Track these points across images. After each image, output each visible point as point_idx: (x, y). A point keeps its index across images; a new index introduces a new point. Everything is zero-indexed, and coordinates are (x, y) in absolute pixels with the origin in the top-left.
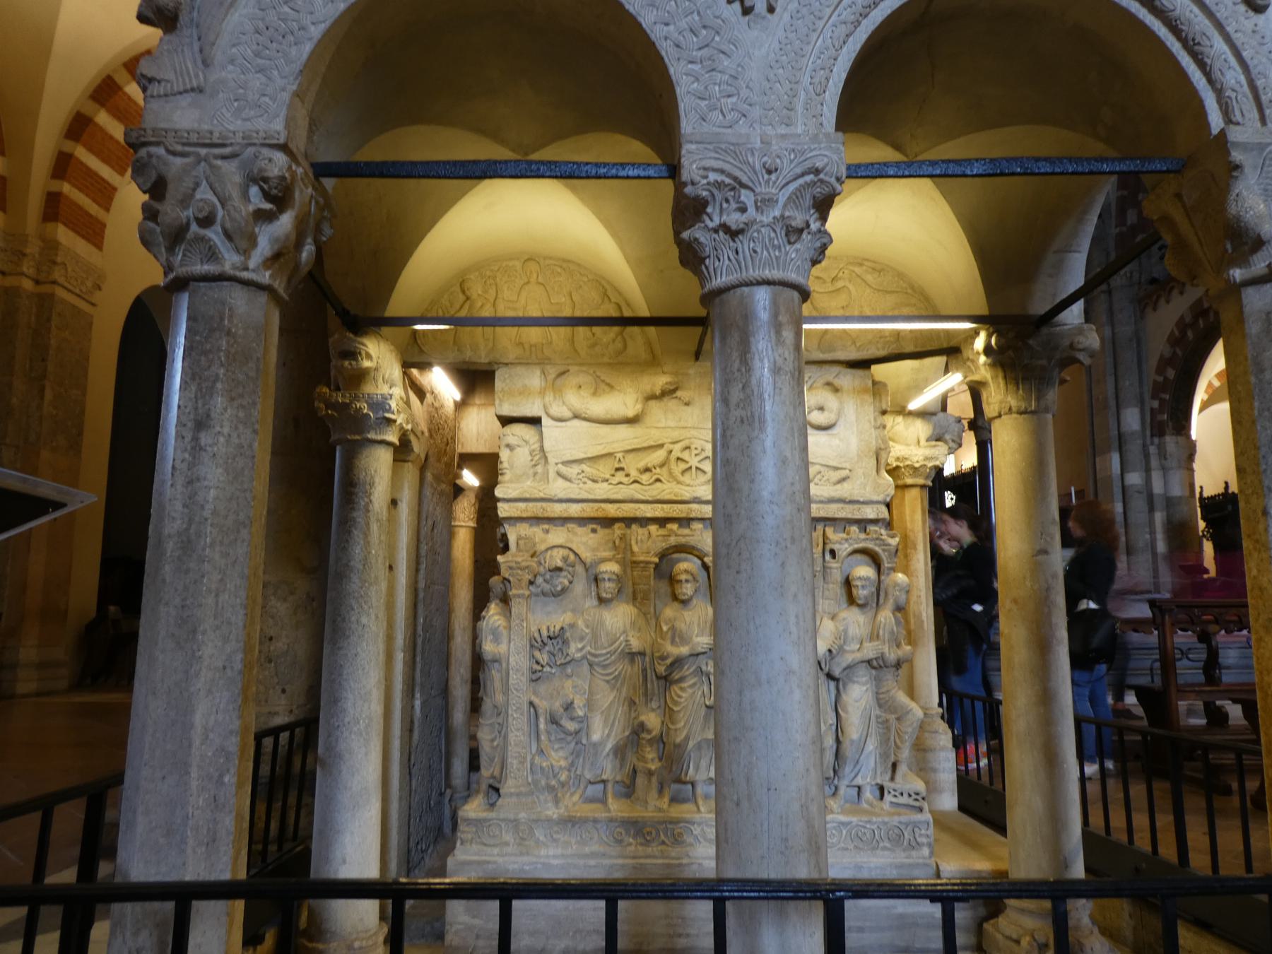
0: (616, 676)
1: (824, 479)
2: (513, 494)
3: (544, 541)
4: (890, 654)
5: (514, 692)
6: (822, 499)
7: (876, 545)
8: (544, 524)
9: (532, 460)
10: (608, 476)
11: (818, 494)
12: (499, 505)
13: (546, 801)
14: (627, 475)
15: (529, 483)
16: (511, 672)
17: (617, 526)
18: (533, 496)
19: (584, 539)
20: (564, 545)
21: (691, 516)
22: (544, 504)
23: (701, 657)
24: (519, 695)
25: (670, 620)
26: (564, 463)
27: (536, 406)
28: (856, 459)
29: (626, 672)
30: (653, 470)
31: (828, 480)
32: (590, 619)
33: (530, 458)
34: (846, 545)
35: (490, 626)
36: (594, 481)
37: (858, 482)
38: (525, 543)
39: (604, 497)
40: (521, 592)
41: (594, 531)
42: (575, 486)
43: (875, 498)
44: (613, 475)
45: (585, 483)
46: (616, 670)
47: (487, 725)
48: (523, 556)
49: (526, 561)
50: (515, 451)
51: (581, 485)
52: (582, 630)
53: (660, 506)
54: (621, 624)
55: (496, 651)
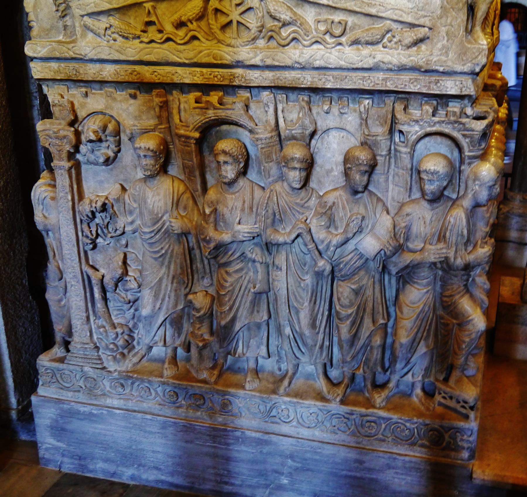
0: (163, 255)
1: (395, 40)
2: (43, 52)
3: (83, 105)
4: (455, 258)
6: (390, 66)
7: (454, 128)
9: (57, 10)
10: (138, 33)
11: (385, 60)
12: (32, 65)
14: (160, 31)
17: (155, 92)
21: (235, 84)
23: (245, 243)
25: (212, 202)
28: (439, 12)
29: (172, 251)
30: (189, 24)
31: (400, 41)
32: (136, 194)
34: (417, 128)
37: (439, 46)
38: (60, 110)
41: (134, 97)
43: (459, 68)
44: (144, 31)
46: (162, 248)
48: (60, 124)
53: (198, 69)
54: (161, 204)
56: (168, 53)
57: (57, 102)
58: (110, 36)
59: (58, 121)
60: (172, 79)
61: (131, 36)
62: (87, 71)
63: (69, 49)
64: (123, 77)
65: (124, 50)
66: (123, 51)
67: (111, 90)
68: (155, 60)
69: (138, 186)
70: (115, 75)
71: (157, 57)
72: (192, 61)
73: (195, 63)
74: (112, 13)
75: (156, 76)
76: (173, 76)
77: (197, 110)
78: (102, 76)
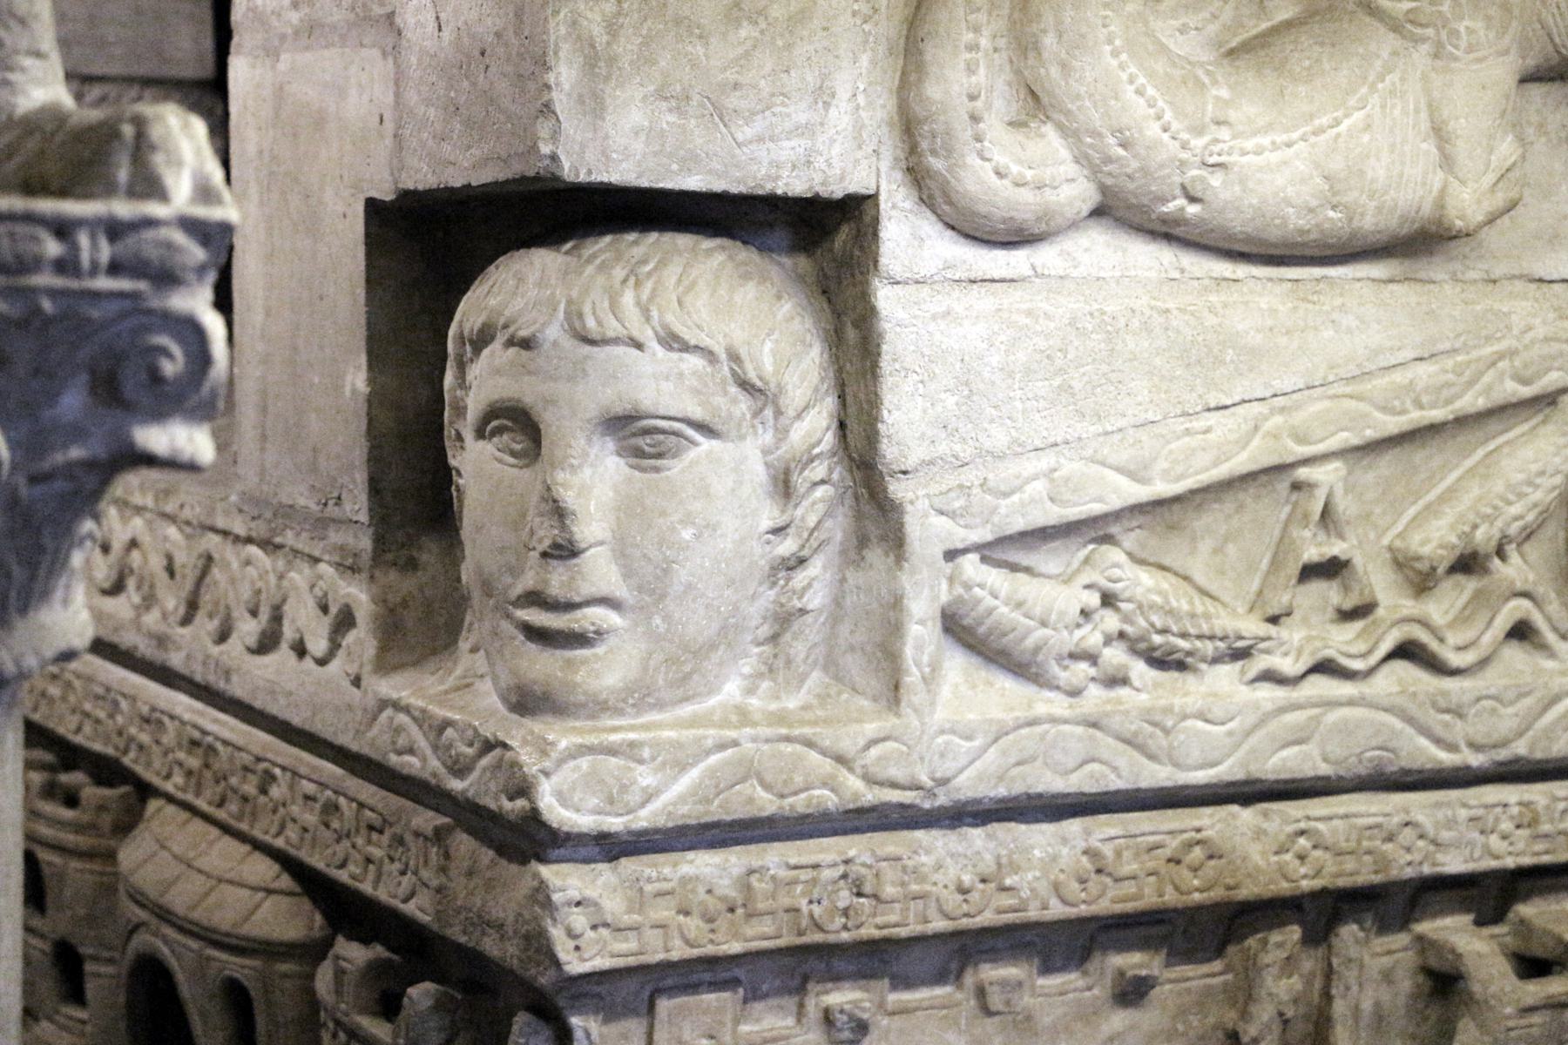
8: (837, 978)
9: (777, 531)
15: (731, 690)
18: (799, 803)
22: (857, 847)
26: (995, 551)
27: (840, 116)
33: (768, 516)
36: (1164, 661)
39: (1226, 770)
41: (1132, 992)
42: (1050, 703)
45: (1117, 680)
50: (675, 468)
51: (1095, 692)
53: (1512, 794)
56: (1398, 724)
58: (1092, 658)
60: (1383, 862)
61: (1208, 648)
62: (922, 879)
63: (841, 760)
64: (1129, 888)
65: (1167, 732)
66: (1159, 741)
67: (1010, 971)
68: (1324, 769)
70: (1083, 881)
71: (1336, 750)
72: (1503, 755)
73: (1517, 760)
74: (1114, 529)
75: (1302, 858)
76: (1389, 847)
77: (1536, 1019)
78: (1008, 901)
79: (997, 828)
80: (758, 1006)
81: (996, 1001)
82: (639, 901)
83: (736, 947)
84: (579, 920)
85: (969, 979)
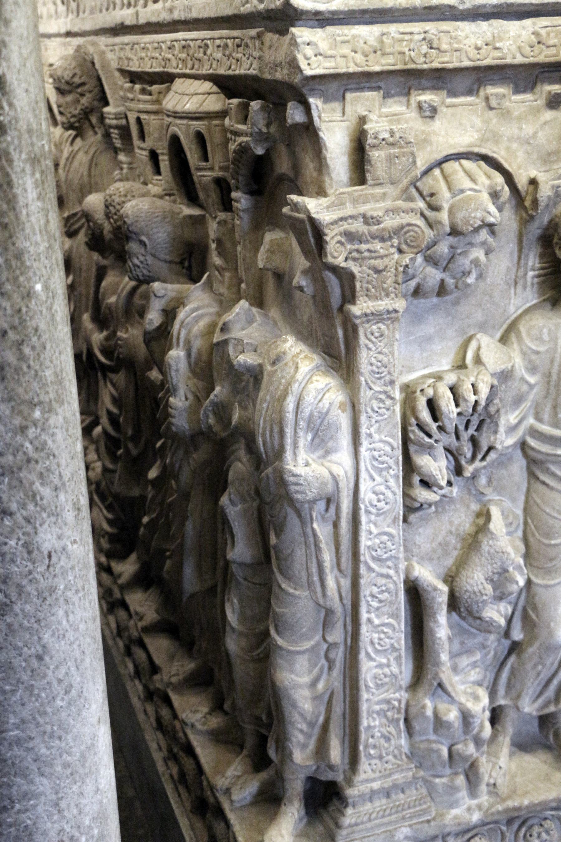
5: (373, 565)
8: (424, 89)
13: (452, 789)
16: (363, 519)
19: (528, 129)
20: (476, 150)
22: (431, 27)
24: (385, 571)
32: (542, 349)
35: (306, 412)
38: (390, 159)
40: (384, 304)
47: (303, 652)
49: (394, 211)
52: (523, 379)
55: (326, 474)
57: (386, 135)
59: (378, 191)
62: (459, 42)
64: (553, 51)
69: (545, 331)
78: (497, 54)
79: (493, 22)
80: (390, 101)
81: (493, 102)
82: (335, 45)
83: (377, 68)
84: (309, 51)
85: (482, 93)
